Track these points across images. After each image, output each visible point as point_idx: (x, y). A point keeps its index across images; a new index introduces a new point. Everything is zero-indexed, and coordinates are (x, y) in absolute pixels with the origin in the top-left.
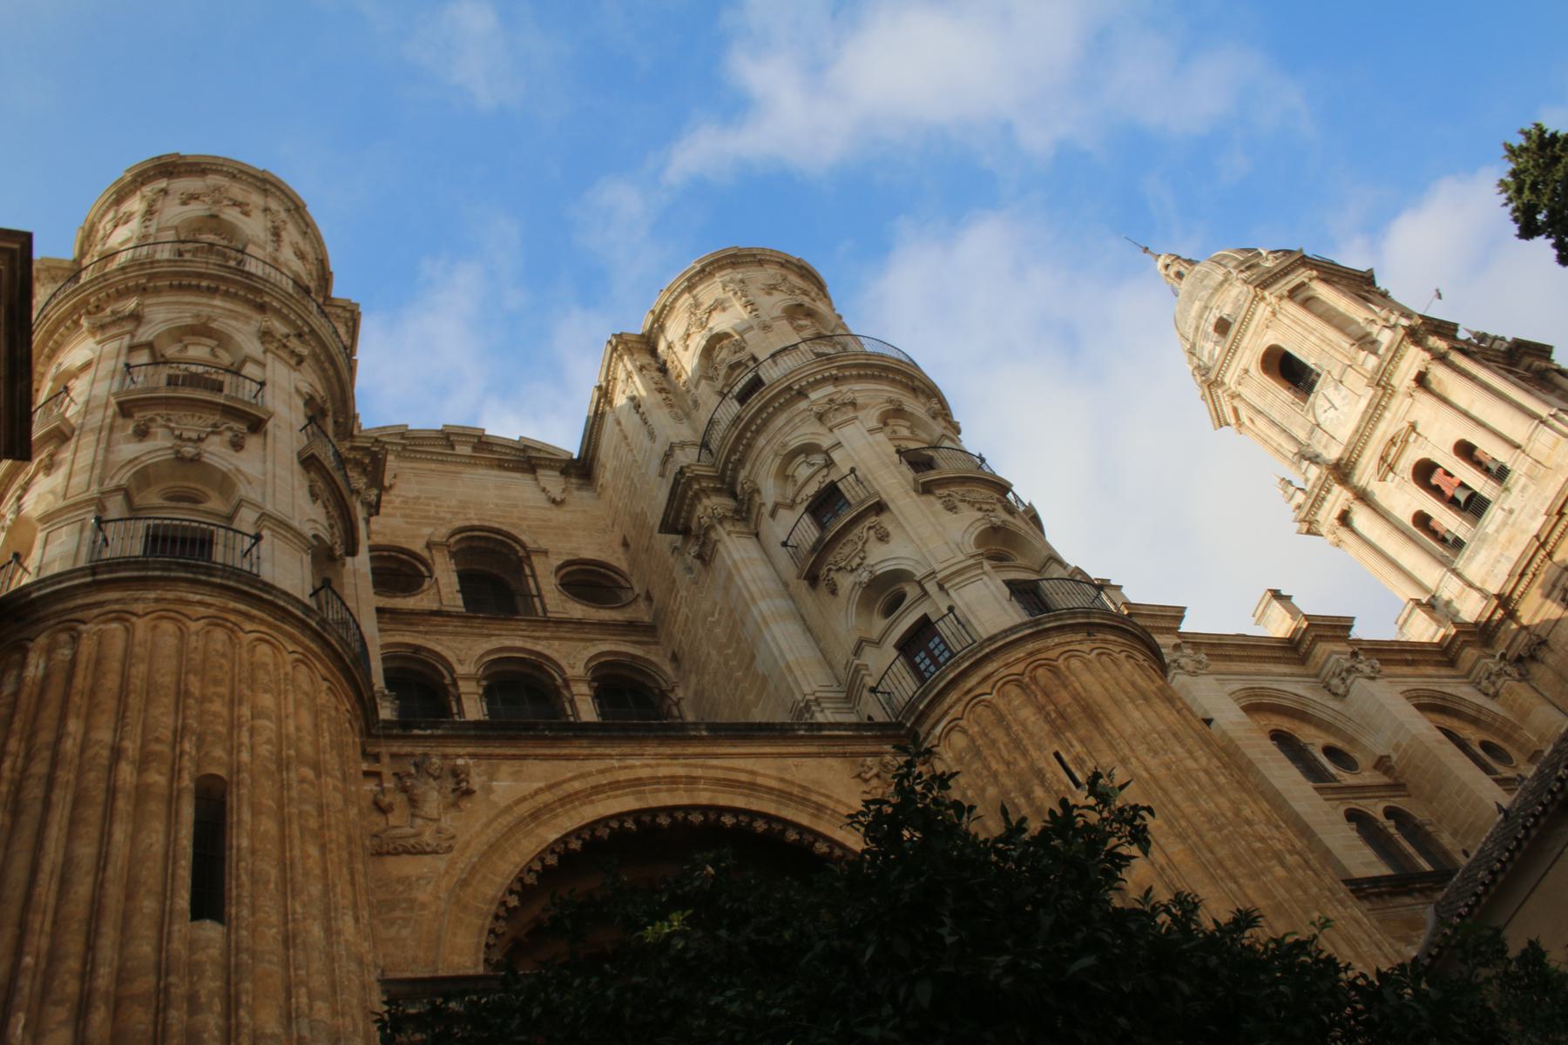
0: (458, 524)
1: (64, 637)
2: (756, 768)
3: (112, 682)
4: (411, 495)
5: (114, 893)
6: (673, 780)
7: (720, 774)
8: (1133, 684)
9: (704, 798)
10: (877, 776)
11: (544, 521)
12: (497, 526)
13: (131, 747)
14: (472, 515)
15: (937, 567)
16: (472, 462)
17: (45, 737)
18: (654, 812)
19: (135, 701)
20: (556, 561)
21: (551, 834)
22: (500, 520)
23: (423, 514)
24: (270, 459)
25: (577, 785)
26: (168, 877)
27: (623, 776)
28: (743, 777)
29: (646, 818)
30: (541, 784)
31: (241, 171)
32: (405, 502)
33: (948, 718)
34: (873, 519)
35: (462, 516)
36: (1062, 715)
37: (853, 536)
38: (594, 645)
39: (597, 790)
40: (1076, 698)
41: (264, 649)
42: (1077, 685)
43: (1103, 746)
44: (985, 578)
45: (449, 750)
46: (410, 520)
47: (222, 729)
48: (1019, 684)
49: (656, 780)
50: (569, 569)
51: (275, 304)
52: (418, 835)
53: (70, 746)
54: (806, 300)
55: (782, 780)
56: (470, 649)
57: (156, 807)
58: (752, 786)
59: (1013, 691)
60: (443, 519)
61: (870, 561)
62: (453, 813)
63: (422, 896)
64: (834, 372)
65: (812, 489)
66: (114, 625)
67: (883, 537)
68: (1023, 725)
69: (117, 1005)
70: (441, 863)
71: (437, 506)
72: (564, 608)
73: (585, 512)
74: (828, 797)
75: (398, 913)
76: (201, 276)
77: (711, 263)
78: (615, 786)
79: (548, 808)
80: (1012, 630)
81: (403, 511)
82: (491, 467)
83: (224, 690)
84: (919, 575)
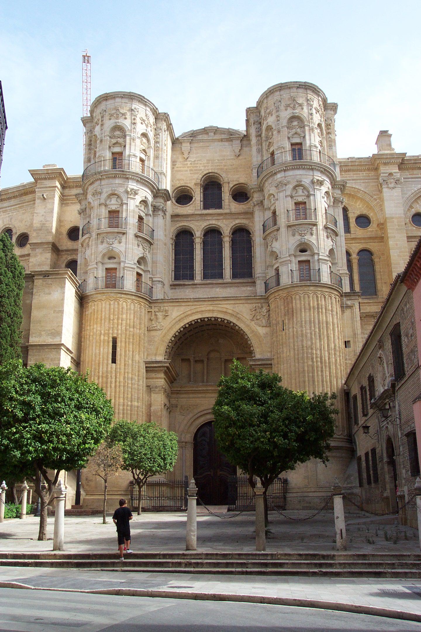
0: (205, 173)
1: (93, 304)
2: (228, 307)
3: (99, 316)
4: (193, 160)
5: (101, 359)
6: (209, 310)
7: (220, 309)
8: (309, 304)
9: (215, 315)
10: (255, 310)
11: (231, 165)
12: (216, 171)
13: (103, 332)
14: (210, 168)
15: (282, 257)
16: (213, 141)
17: (92, 327)
18: (204, 318)
19: (103, 322)
20: (231, 186)
21: (182, 324)
22: (218, 167)
23: (196, 168)
24: (127, 243)
25: (189, 312)
26: (108, 357)
27: (199, 310)
28: (225, 310)
29: (203, 319)
30: (182, 313)
31: (124, 95)
32: (191, 164)
33: (272, 300)
34: (275, 233)
35: (207, 168)
36: (288, 310)
37: (272, 235)
38: (234, 221)
39: (193, 313)
40: (292, 307)
41: (125, 303)
42: (294, 304)
43: (291, 323)
44: (290, 265)
45: (165, 305)
46: (191, 172)
47: (116, 326)
48: (284, 299)
49: (206, 311)
50: (236, 187)
51: (130, 177)
52: (156, 326)
53: (95, 330)
54: (297, 111)
55: (233, 311)
56: (201, 226)
57: (106, 344)
58: (226, 312)
59: (282, 300)
60: (201, 170)
61: (273, 246)
62: (164, 320)
63: (156, 339)
64: (284, 168)
65: (272, 208)
66: (99, 302)
67: (277, 240)
68: (281, 310)
69: (102, 377)
70: (159, 332)
71: (200, 164)
72: (229, 205)
73: (245, 159)
74: (242, 315)
75: (152, 343)
76: (112, 174)
77: (273, 89)
78: (197, 312)
79: (182, 318)
80: (285, 286)
81: (190, 168)
82: (219, 141)
83: (117, 317)
84: (279, 256)
